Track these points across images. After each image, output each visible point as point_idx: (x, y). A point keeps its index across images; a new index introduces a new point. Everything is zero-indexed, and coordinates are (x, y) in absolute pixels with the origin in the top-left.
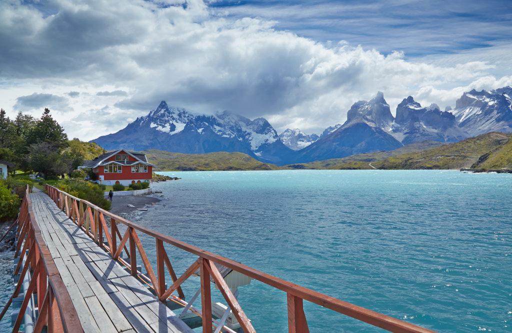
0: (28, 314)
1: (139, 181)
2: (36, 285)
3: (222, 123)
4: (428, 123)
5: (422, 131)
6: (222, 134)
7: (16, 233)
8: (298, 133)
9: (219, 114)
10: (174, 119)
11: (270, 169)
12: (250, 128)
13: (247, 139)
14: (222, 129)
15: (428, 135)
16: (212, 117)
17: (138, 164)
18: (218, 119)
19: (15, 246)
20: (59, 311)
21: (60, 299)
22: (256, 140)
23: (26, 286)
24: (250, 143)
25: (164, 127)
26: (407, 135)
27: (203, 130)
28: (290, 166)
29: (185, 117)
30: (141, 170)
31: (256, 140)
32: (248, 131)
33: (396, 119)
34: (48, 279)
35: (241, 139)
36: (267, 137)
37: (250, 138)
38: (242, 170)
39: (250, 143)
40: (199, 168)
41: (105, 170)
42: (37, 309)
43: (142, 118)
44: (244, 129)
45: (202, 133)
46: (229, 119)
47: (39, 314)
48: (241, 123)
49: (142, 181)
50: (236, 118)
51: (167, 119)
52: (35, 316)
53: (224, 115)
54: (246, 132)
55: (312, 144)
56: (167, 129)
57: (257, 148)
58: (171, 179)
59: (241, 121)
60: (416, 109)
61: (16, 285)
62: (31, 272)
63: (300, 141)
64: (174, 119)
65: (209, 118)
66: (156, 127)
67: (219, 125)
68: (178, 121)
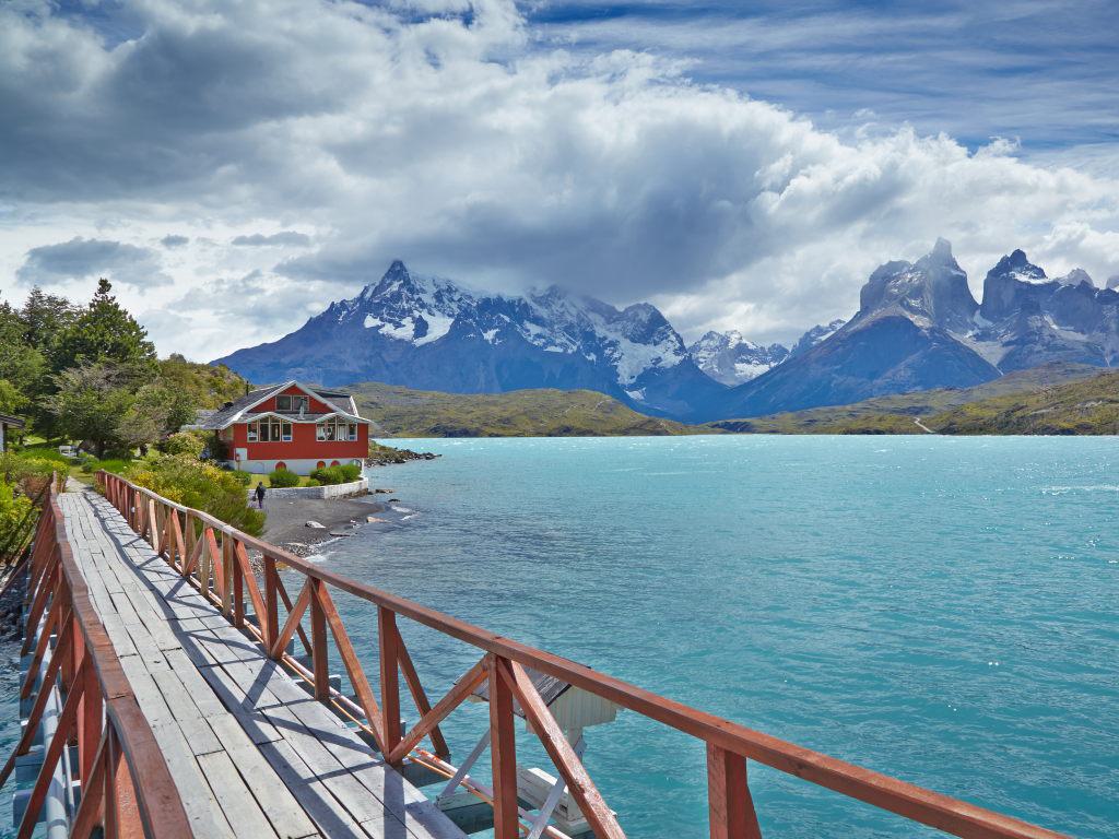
0: (56, 797)
1: (335, 463)
2: (75, 724)
3: (545, 316)
4: (1062, 319)
5: (1047, 338)
6: (545, 345)
7: (23, 592)
8: (737, 342)
9: (537, 294)
10: (423, 306)
11: (667, 433)
12: (616, 330)
13: (609, 358)
14: (546, 331)
15: (1064, 348)
16: (520, 300)
17: (332, 420)
18: (535, 306)
19: (21, 626)
20: (132, 788)
21: (136, 756)
22: (631, 359)
23: (51, 725)
24: (616, 367)
25: (398, 325)
26: (1011, 347)
27: (497, 335)
28: (717, 426)
29: (452, 300)
30: (342, 435)
31: (631, 359)
32: (612, 337)
33: (984, 309)
34: (104, 709)
35: (592, 357)
36: (658, 351)
37: (616, 355)
38: (595, 435)
39: (616, 367)
40: (488, 430)
41: (252, 435)
42: (78, 783)
43: (342, 303)
44: (600, 332)
45: (494, 341)
46: (562, 305)
47: (83, 796)
48: (592, 316)
49: (344, 462)
50: (581, 305)
52: (72, 802)
53: (549, 295)
54: (605, 338)
55: (772, 370)
56: (407, 330)
57: (634, 380)
58: (417, 456)
59: (592, 311)
60: (1033, 282)
61: (25, 723)
62: (63, 691)
63: (742, 361)
64: (423, 306)
65: (511, 304)
66: (379, 327)
67: (537, 321)
68: (434, 310)
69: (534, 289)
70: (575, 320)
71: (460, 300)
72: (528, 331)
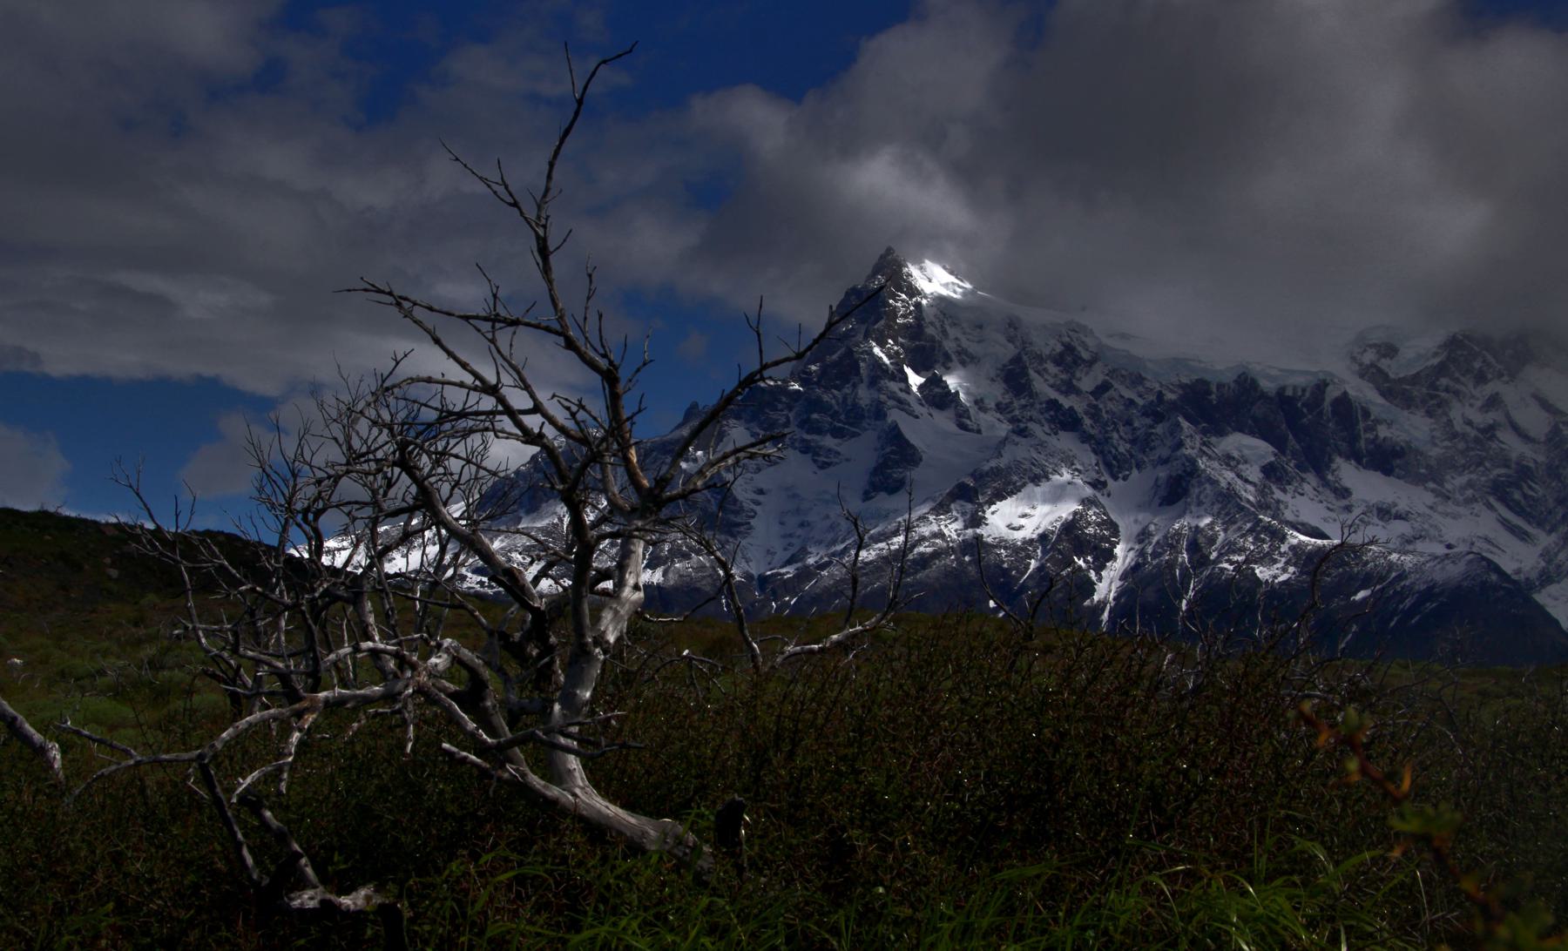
16: (1321, 387)
51: (864, 395)
53: (1441, 369)
65: (1284, 402)
69: (1389, 351)
70: (1535, 456)
71: (1103, 388)
72: (1343, 493)
